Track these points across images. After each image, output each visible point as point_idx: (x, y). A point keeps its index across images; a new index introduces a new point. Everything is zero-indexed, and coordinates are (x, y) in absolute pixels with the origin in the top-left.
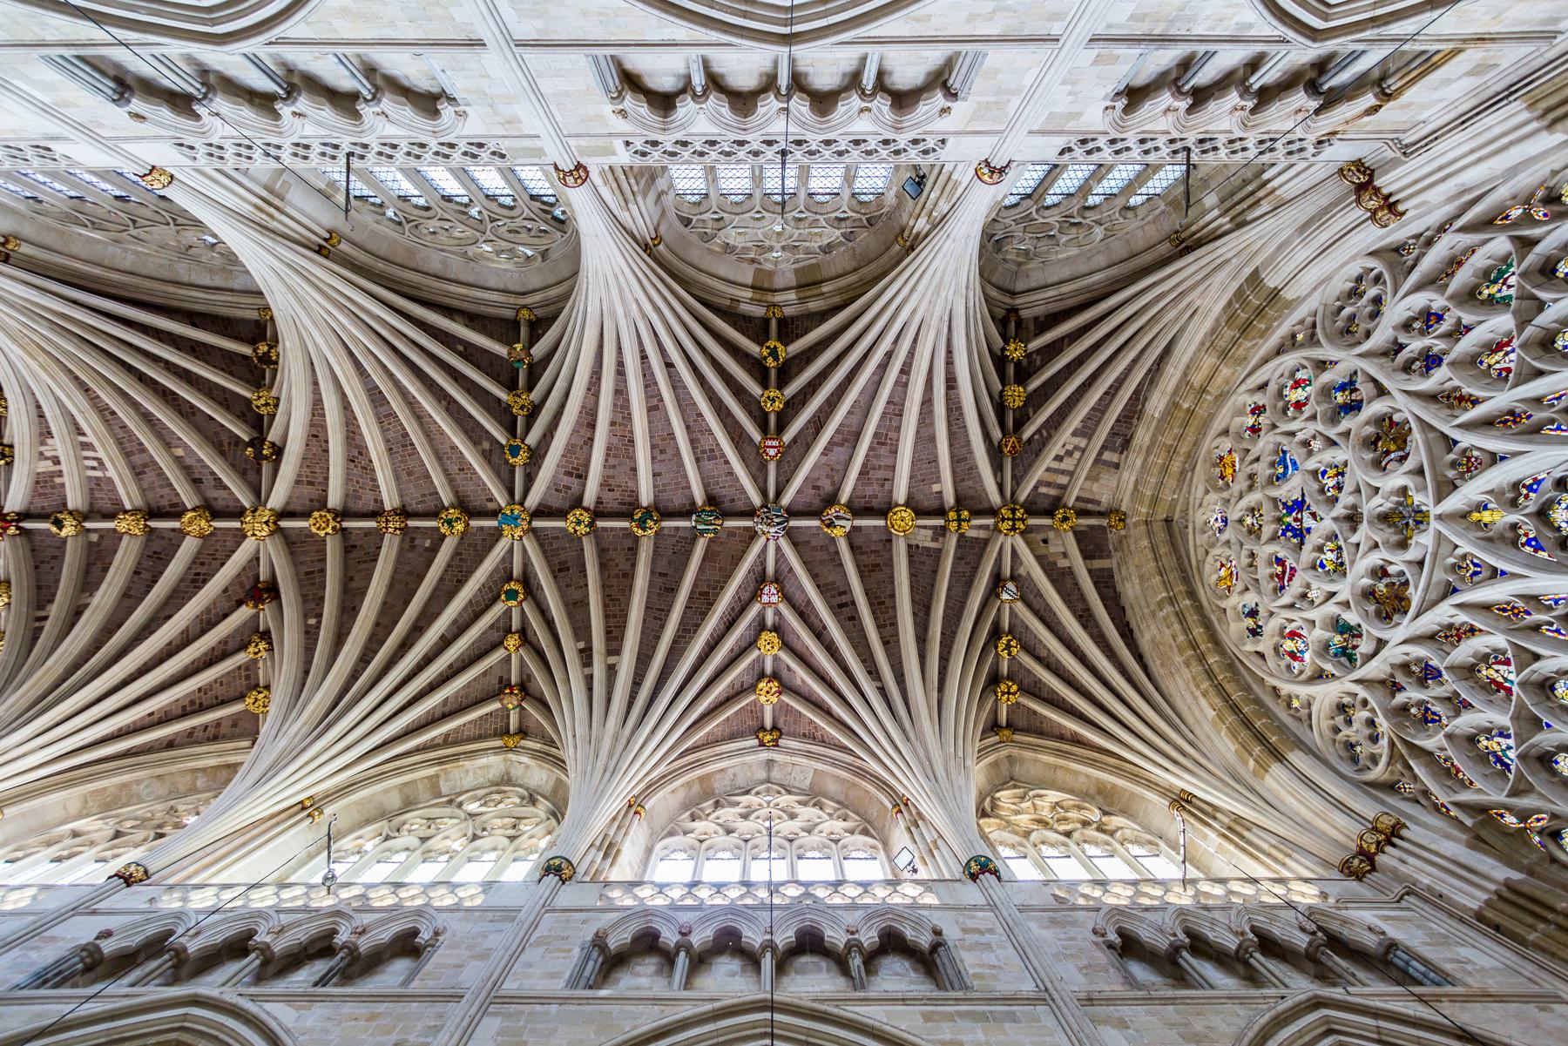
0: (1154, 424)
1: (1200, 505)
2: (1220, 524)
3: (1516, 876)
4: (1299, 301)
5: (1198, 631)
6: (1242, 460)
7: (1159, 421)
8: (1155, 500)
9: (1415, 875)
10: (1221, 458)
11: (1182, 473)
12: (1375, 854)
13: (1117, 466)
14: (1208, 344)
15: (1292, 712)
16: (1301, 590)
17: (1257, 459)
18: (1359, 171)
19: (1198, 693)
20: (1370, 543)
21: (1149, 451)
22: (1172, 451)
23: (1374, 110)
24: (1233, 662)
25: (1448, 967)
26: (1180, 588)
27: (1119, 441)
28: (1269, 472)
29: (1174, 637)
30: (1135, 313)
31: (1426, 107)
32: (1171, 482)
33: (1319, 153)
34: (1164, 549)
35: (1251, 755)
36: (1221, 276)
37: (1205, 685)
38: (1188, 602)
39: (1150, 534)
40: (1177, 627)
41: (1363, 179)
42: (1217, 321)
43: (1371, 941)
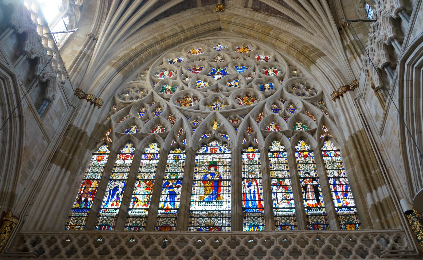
0: (264, 21)
1: (227, 41)
2: (218, 48)
4: (309, 71)
5: (170, 41)
6: (245, 54)
7: (265, 23)
8: (229, 23)
9: (81, 110)
10: (247, 48)
11: (242, 33)
12: (86, 99)
13: (246, 7)
14: (297, 39)
15: (139, 75)
16: (189, 75)
17: (245, 60)
18: (354, 86)
19: (142, 42)
20: (207, 95)
21: (252, 19)
22: (252, 28)
23: (373, 87)
24: (158, 55)
25: (48, 116)
26: (189, 34)
27: (257, 7)
28: (239, 64)
29: (166, 33)
30: (315, 10)
31: (370, 104)
32: (237, 29)
33: (364, 72)
34: (206, 27)
35: (118, 61)
36: (325, 43)
37: (146, 45)
38: (183, 37)
39: (214, 21)
40: (171, 33)
41: (351, 88)
42: (307, 42)
43: (49, 95)
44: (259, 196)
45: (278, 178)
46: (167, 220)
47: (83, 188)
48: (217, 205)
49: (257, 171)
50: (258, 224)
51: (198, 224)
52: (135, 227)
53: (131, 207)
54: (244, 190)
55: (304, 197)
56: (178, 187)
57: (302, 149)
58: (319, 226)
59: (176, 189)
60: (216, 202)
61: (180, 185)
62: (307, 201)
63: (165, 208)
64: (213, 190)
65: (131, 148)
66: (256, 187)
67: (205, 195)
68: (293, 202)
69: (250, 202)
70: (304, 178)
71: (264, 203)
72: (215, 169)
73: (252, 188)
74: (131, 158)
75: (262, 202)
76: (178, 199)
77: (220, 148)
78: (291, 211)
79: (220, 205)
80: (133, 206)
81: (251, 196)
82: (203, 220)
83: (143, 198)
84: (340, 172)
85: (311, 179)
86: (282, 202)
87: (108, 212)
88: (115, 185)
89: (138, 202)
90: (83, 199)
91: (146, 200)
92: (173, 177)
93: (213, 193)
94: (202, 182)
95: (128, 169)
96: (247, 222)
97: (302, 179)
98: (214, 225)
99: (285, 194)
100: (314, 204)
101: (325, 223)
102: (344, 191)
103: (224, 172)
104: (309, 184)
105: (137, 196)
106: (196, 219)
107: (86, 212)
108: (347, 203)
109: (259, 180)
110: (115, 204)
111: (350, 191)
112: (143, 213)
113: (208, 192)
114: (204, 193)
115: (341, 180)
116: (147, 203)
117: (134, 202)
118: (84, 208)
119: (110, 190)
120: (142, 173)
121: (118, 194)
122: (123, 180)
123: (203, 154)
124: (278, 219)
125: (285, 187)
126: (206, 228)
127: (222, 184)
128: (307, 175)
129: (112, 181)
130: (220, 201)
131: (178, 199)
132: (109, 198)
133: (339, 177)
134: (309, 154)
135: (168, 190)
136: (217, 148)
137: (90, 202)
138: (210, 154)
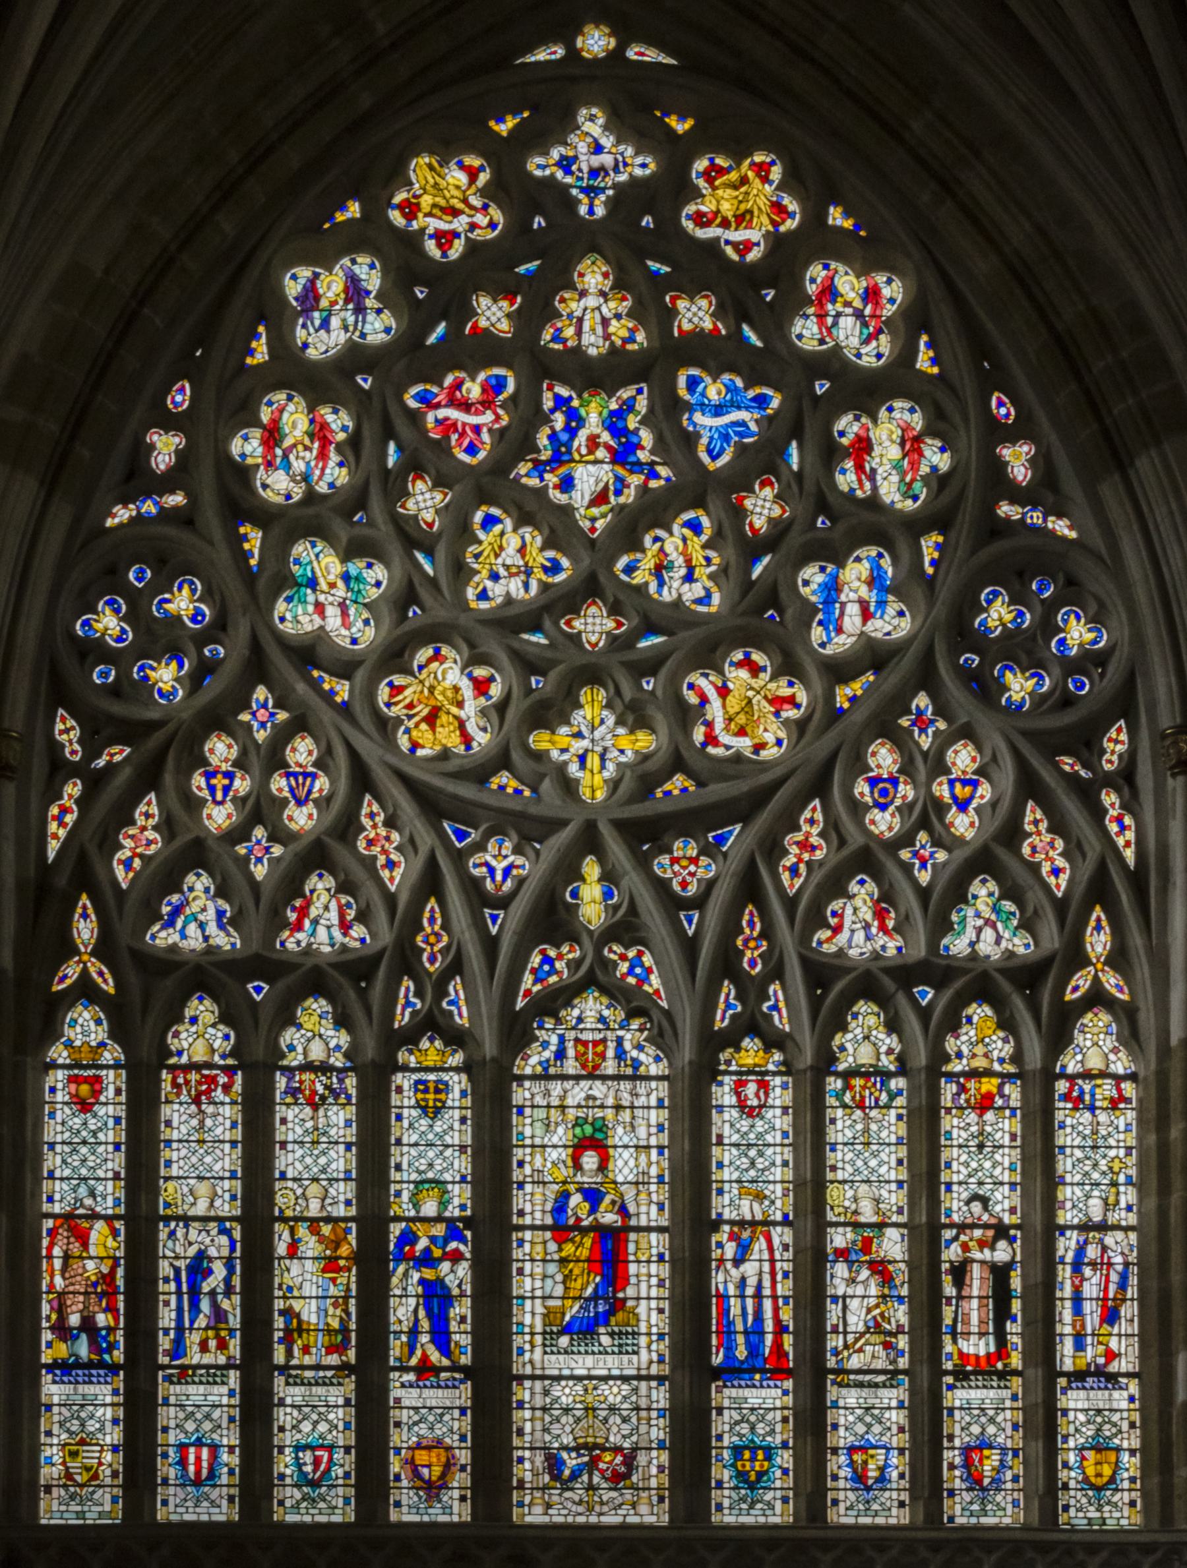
3: (11, 974)
44: (776, 1310)
45: (856, 1225)
46: (431, 1418)
47: (58, 1264)
48: (616, 1349)
49: (775, 1182)
50: (769, 1439)
51: (547, 1438)
52: (313, 1448)
53: (279, 1356)
54: (721, 1277)
55: (948, 1320)
56: (456, 1257)
57: (974, 1056)
58: (986, 1452)
59: (445, 1266)
60: (612, 1334)
61: (462, 1247)
62: (960, 1341)
63: (414, 1361)
64: (598, 1279)
65: (214, 1025)
66: (766, 1267)
67: (568, 1303)
68: (903, 1342)
69: (740, 1339)
70: (962, 1227)
71: (795, 1345)
72: (603, 1167)
73: (749, 1269)
74: (227, 1088)
75: (788, 1341)
76: (463, 1320)
77: (620, 1041)
78: (892, 1386)
79: (627, 1353)
80: (289, 1354)
81: (744, 1309)
82: (564, 1420)
83: (322, 1314)
84: (1111, 1200)
85: (990, 1233)
86: (863, 1341)
87: (194, 1383)
88: (190, 1244)
89: (305, 1335)
90: (74, 1320)
91: (335, 1324)
92: (430, 1208)
93: (596, 1290)
94: (548, 1235)
95: (227, 1159)
96: (727, 1428)
97: (954, 1231)
98: (607, 1439)
99: (877, 1306)
100: (982, 1353)
101: (1009, 1445)
102: (1111, 1295)
103: (637, 1183)
104: (978, 1255)
105: (297, 1305)
106: (538, 1413)
107: (106, 1383)
108: (1111, 1355)
109: (779, 1229)
110: (212, 1344)
111: (1132, 1300)
112: (332, 1384)
113: (578, 1285)
114: (559, 1290)
115: (1109, 1240)
116: (339, 1338)
117: (288, 1331)
118: (90, 1365)
119: (177, 1271)
120: (294, 1180)
121: (213, 1293)
122: (220, 1220)
123: (545, 1077)
124: (842, 1421)
125: (880, 1269)
126: (579, 1456)
127: (631, 1248)
128: (976, 1207)
129: (173, 1224)
130: (627, 1333)
131: (463, 1320)
132: (180, 1310)
133: (1103, 1227)
134: (1000, 1087)
135: (416, 1276)
136: (604, 1041)
137: (108, 1334)
138: (577, 1078)
